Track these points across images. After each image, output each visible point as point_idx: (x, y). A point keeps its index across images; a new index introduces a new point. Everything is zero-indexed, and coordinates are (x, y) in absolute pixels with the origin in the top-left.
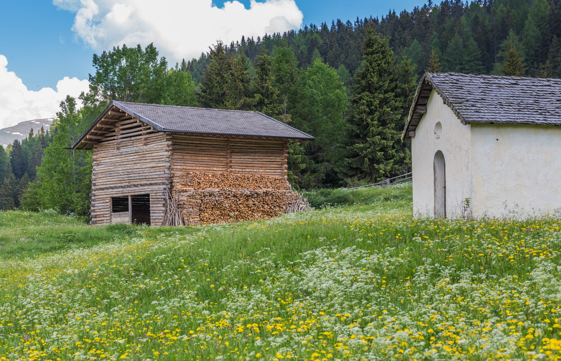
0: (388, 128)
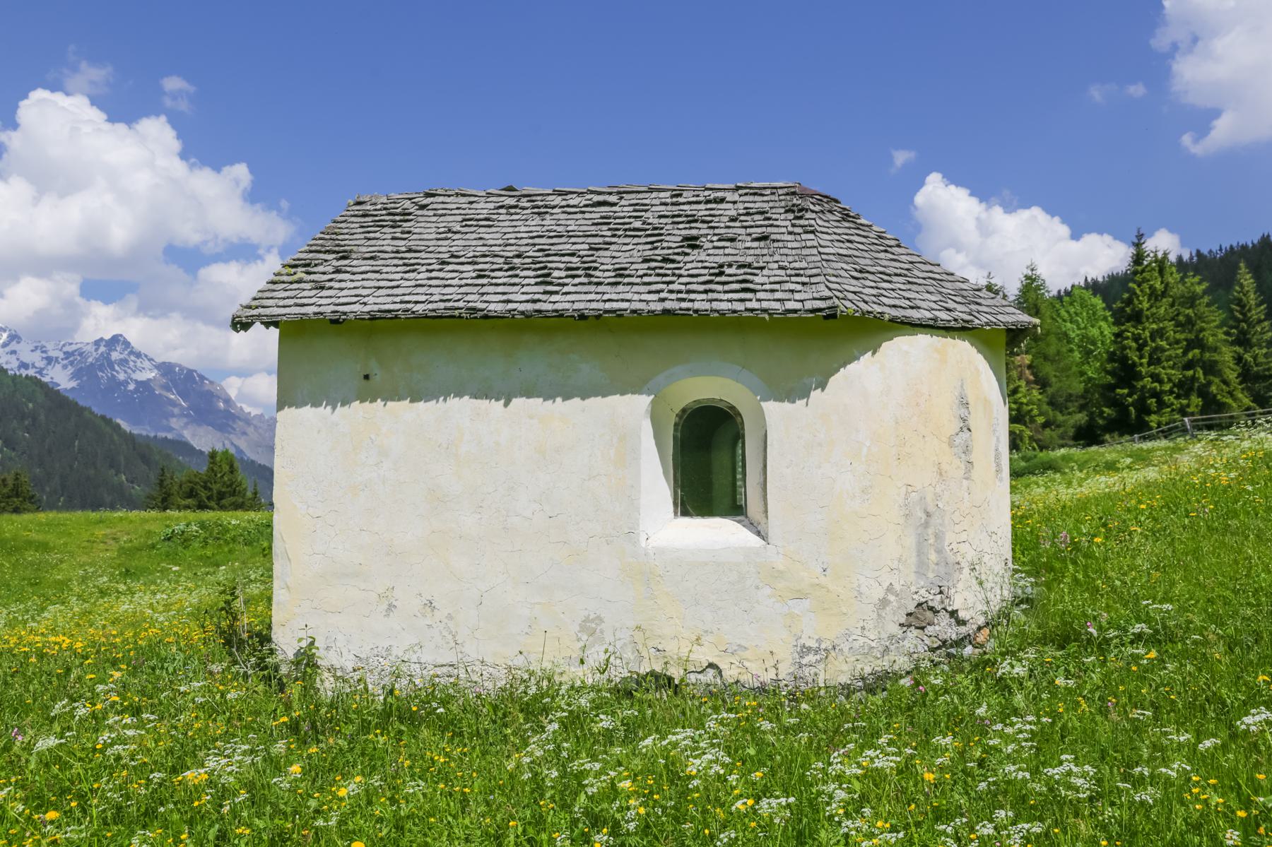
0: (1164, 368)
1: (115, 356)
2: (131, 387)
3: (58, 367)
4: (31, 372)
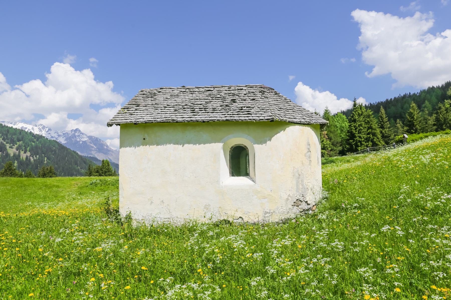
1: (76, 134)
2: (81, 143)
3: (61, 137)
4: (54, 139)
